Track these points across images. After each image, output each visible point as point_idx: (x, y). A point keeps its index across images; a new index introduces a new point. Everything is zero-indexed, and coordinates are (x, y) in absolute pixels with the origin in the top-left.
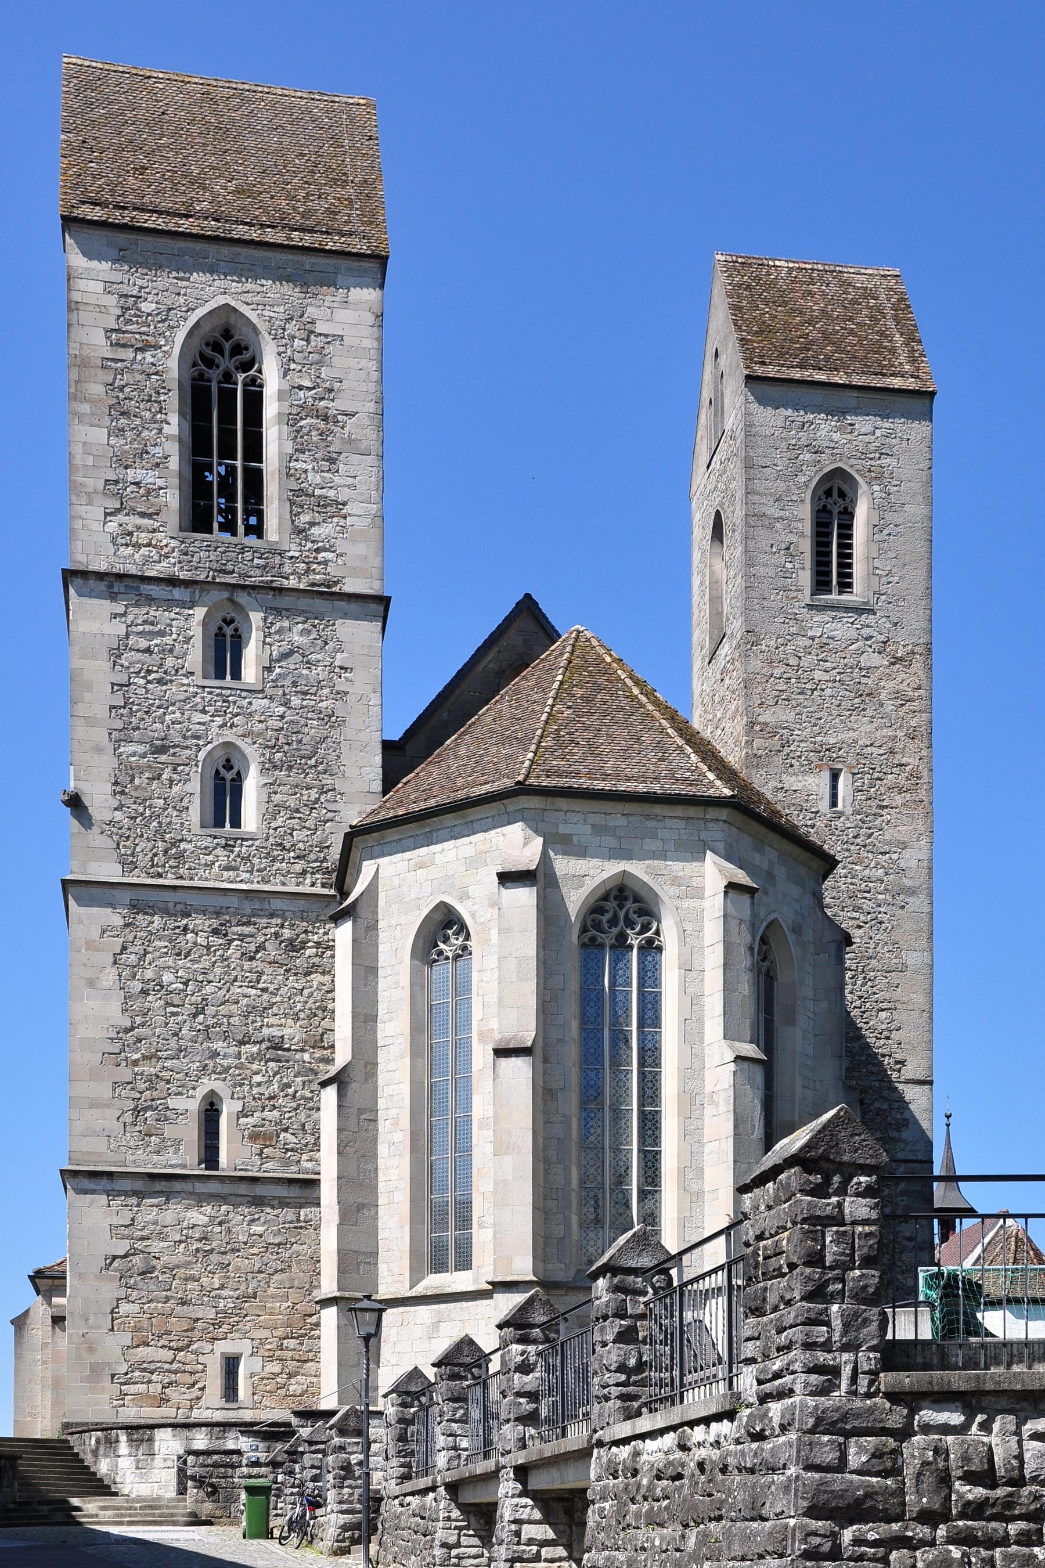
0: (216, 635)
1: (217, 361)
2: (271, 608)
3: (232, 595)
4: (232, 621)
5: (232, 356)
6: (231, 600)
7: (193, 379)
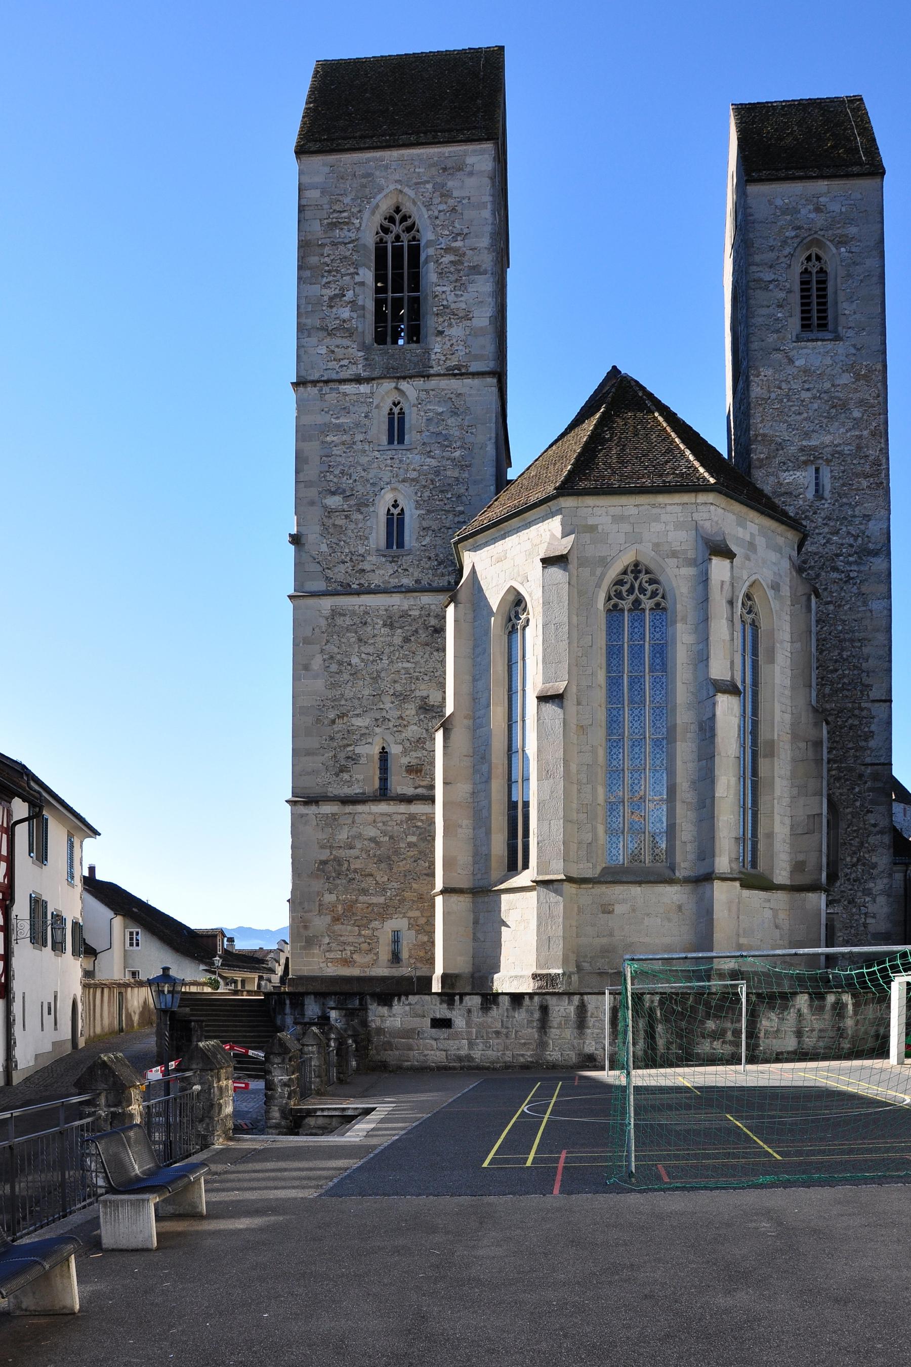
0: (389, 414)
1: (391, 229)
2: (422, 390)
3: (397, 384)
4: (399, 403)
5: (401, 223)
6: (396, 388)
7: (376, 243)
